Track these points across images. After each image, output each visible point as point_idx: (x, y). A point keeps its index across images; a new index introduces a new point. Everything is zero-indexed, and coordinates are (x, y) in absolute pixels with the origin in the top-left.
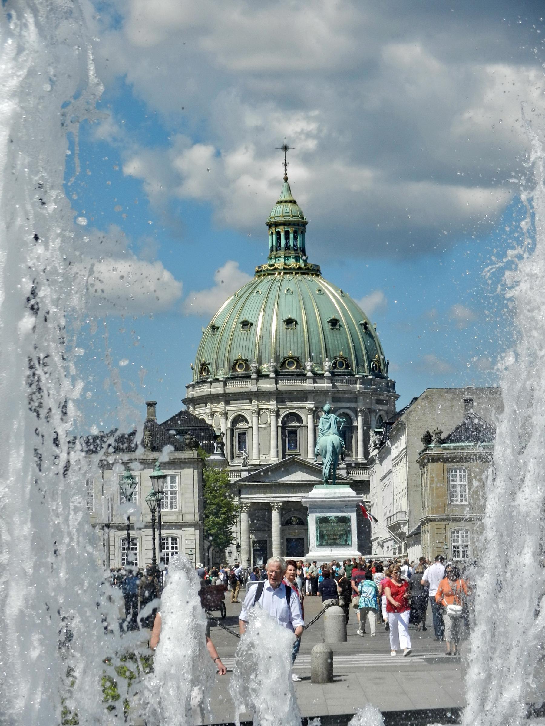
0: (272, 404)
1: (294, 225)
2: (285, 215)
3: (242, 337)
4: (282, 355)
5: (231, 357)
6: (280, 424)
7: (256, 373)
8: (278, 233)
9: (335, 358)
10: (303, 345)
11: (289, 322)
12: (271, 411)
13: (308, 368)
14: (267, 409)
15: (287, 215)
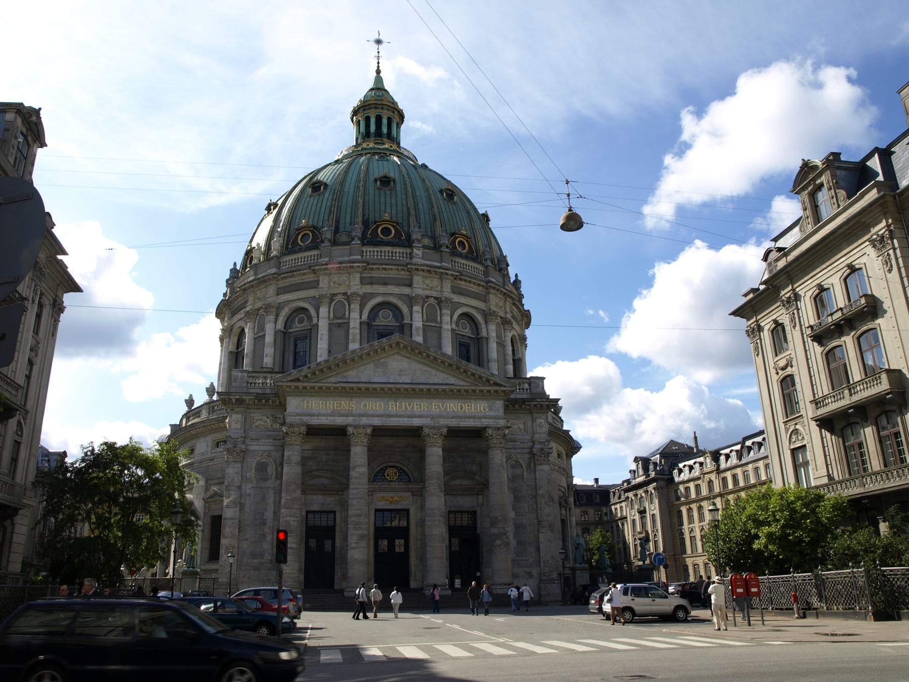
0: (355, 285)
1: (388, 109)
2: (376, 98)
3: (311, 202)
4: (371, 219)
5: (292, 227)
6: (365, 317)
7: (329, 241)
8: (367, 120)
9: (453, 234)
10: (405, 210)
11: (386, 181)
12: (348, 297)
13: (414, 236)
14: (345, 294)
15: (379, 98)
